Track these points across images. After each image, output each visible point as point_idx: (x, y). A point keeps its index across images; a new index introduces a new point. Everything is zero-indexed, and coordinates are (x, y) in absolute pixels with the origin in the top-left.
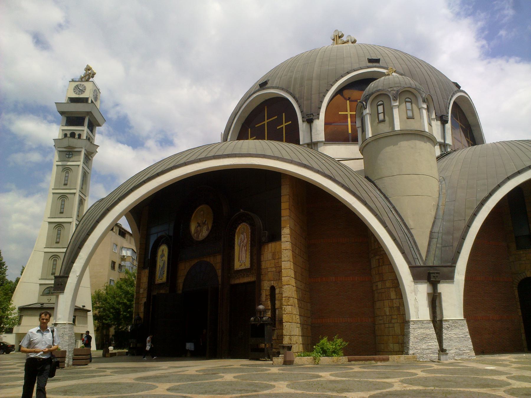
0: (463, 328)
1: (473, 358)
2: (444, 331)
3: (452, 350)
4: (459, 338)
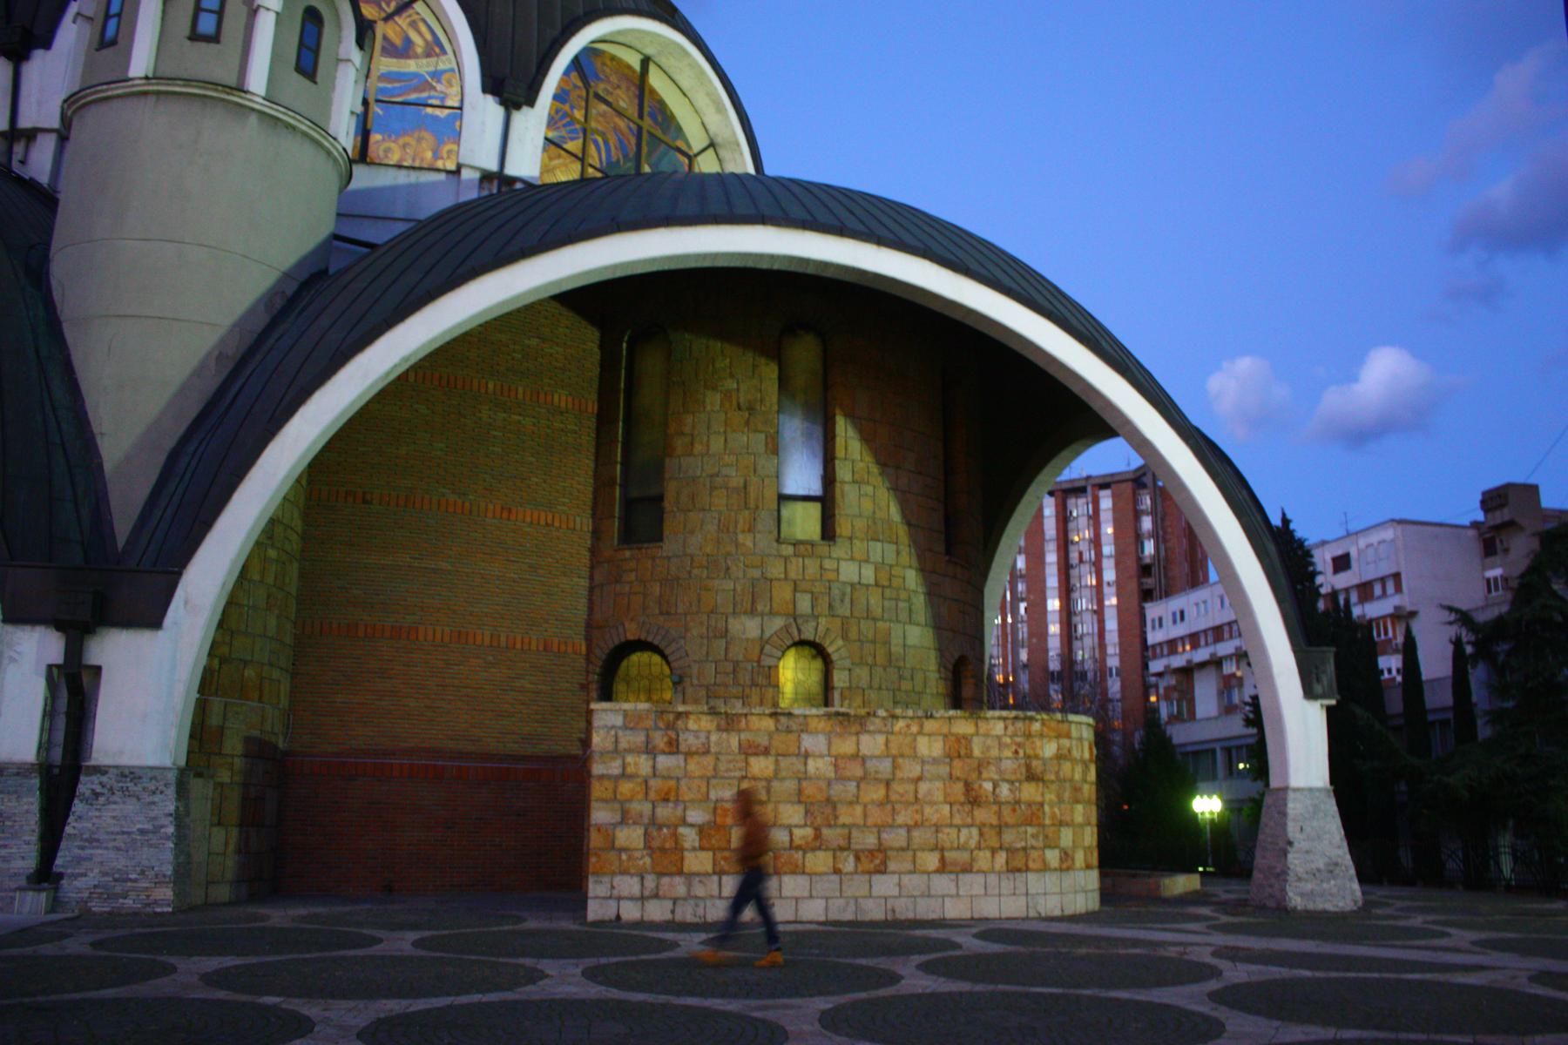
0: (156, 799)
1: (158, 910)
2: (78, 807)
3: (85, 875)
4: (128, 833)
